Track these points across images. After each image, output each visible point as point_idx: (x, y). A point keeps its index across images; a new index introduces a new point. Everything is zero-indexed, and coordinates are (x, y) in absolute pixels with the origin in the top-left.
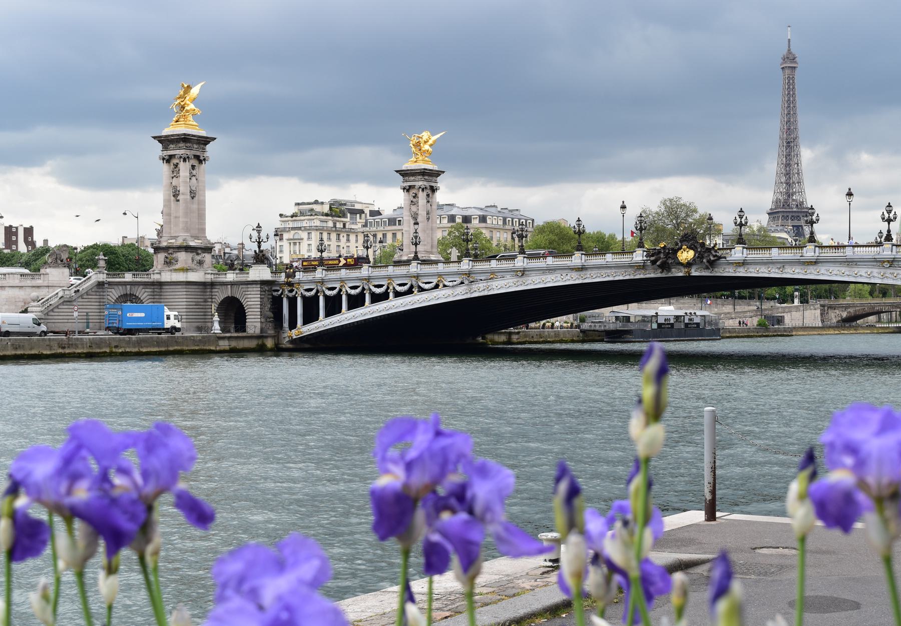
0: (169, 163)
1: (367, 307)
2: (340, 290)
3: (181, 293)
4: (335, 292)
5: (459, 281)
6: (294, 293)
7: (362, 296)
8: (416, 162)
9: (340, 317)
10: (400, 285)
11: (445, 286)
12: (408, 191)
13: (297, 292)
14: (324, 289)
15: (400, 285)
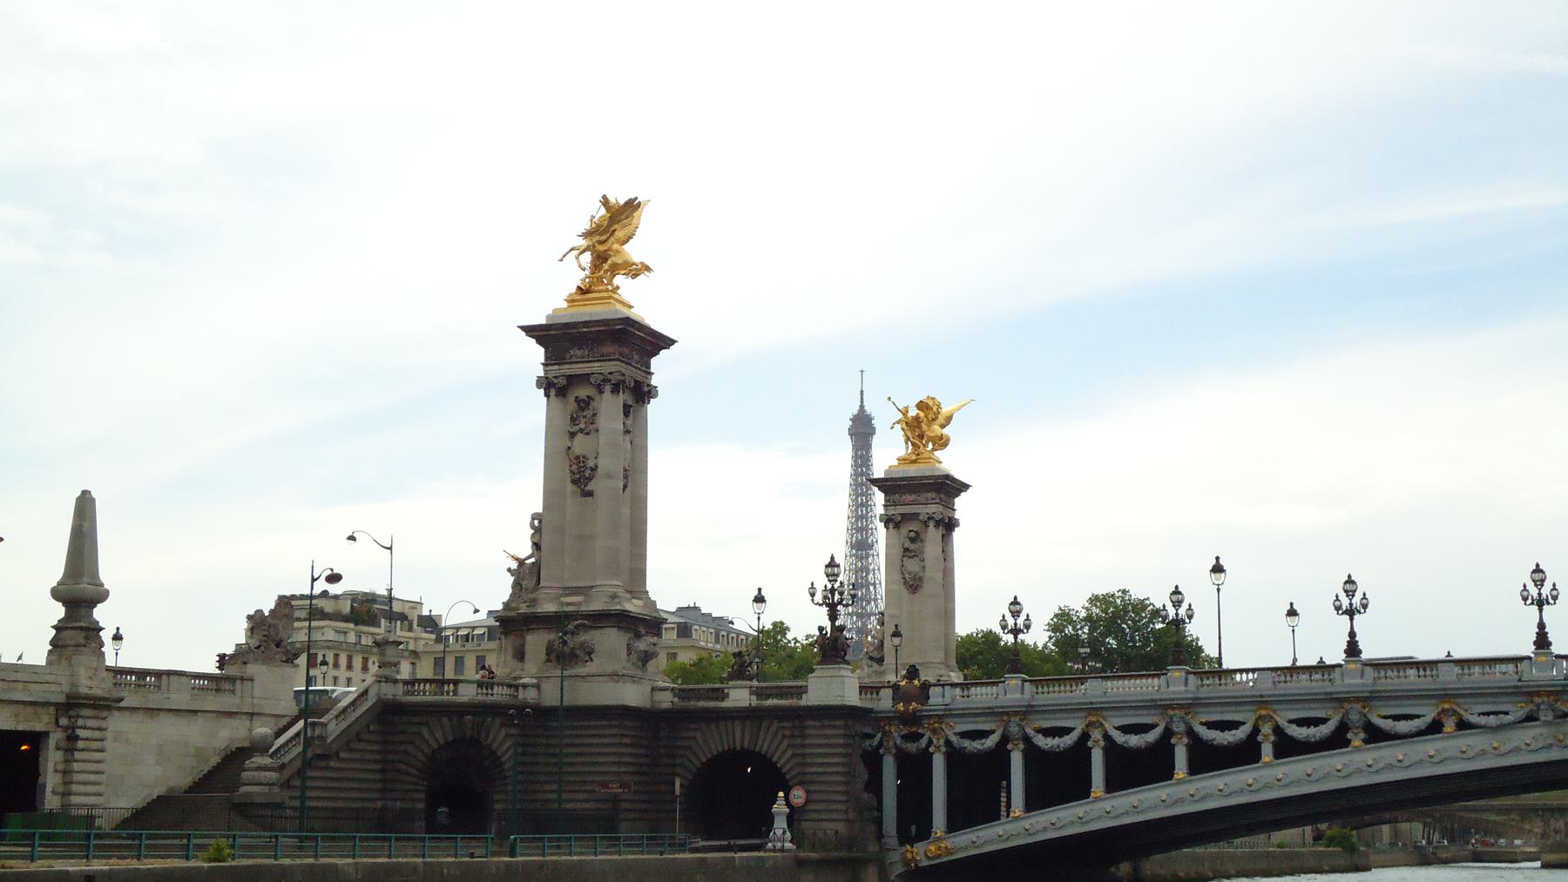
0: (564, 396)
1: (1180, 782)
2: (1085, 736)
3: (606, 741)
4: (1068, 740)
5: (1517, 711)
6: (924, 742)
7: (1163, 749)
8: (914, 462)
9: (1087, 808)
10: (1301, 722)
11: (1463, 725)
12: (897, 526)
13: (930, 742)
14: (1030, 731)
15: (1301, 722)
